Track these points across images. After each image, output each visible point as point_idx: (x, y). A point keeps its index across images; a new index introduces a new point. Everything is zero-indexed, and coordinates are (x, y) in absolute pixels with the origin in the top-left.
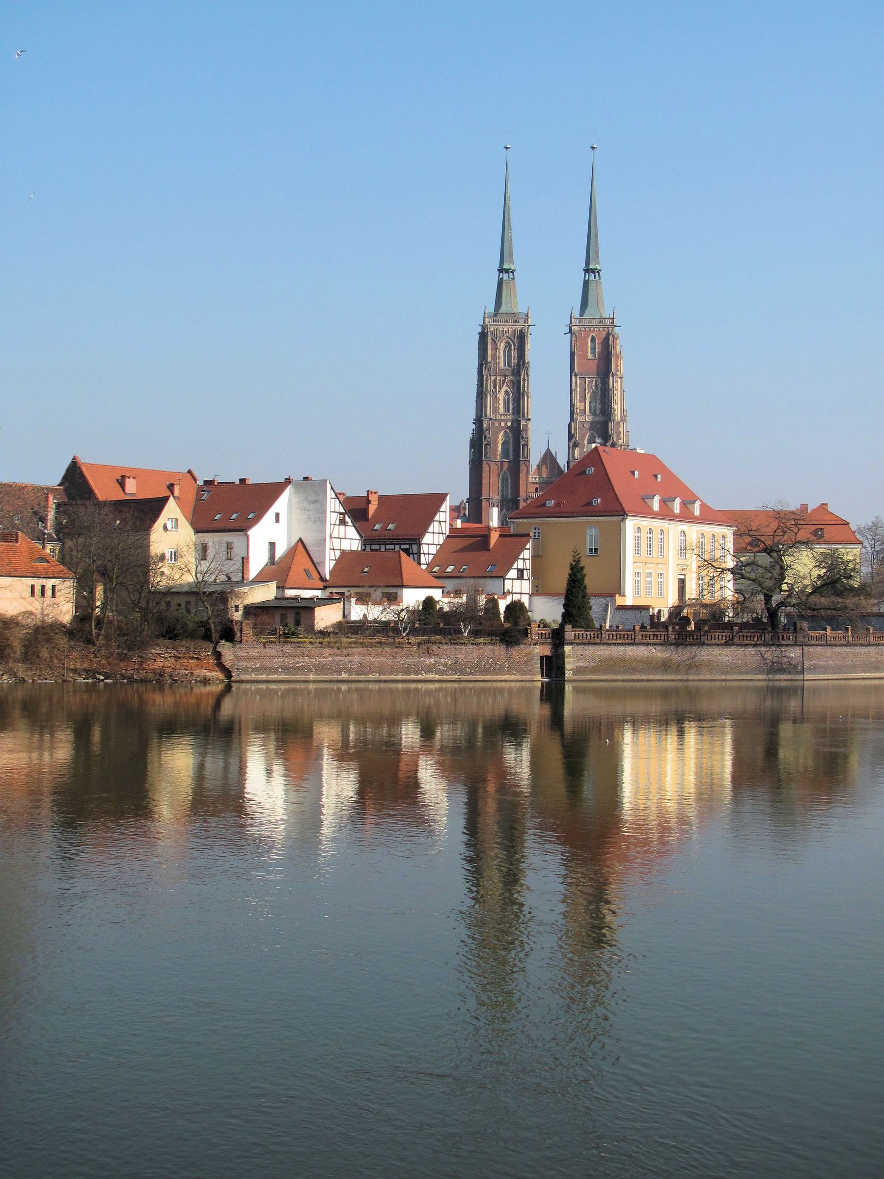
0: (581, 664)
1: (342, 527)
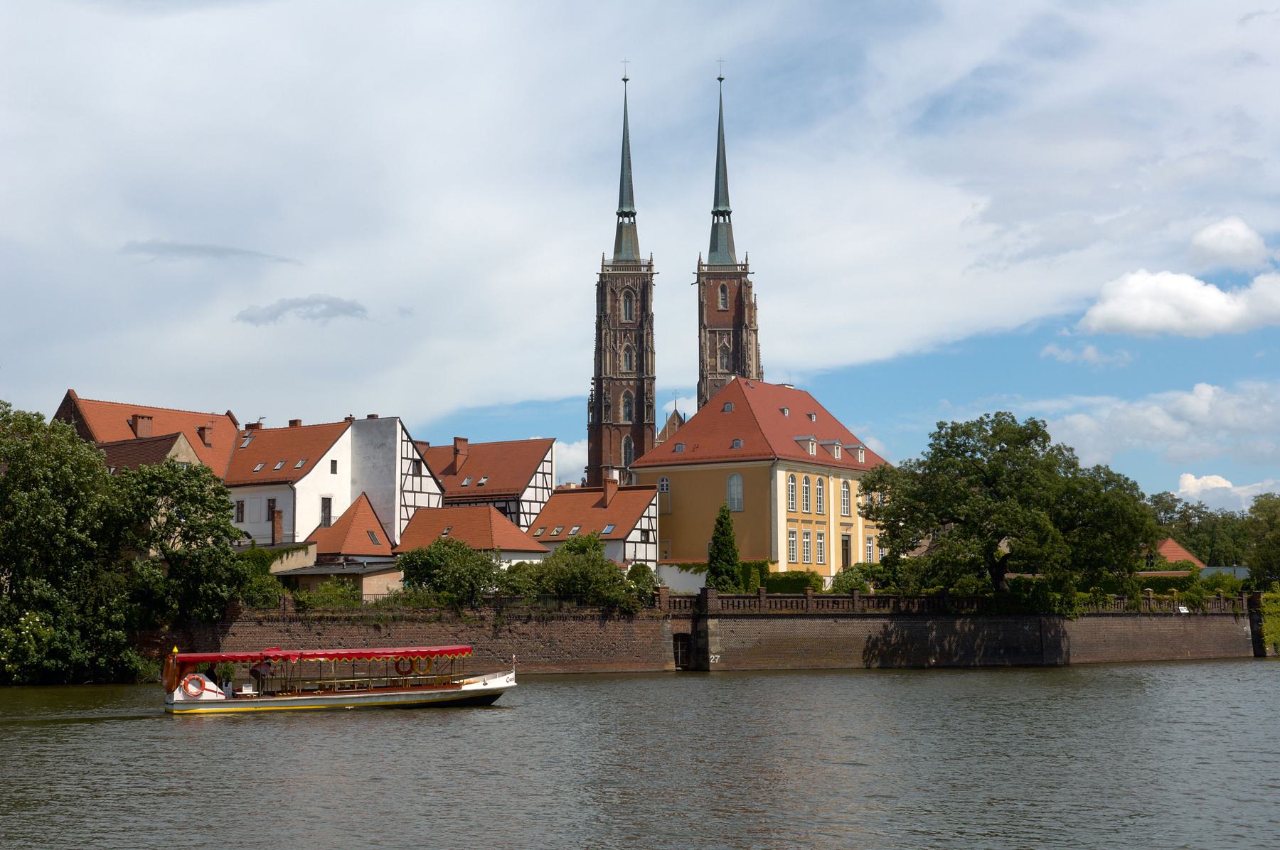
0: (732, 645)
1: (417, 479)
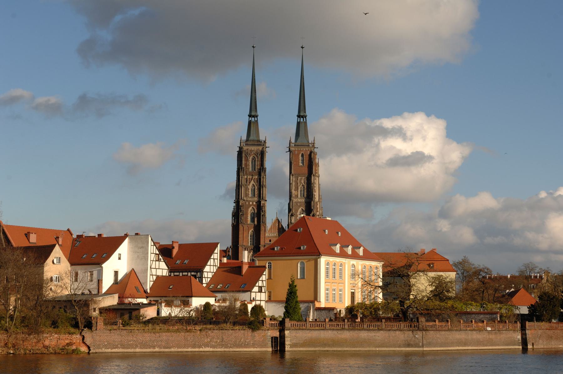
0: (294, 341)
1: (157, 263)
